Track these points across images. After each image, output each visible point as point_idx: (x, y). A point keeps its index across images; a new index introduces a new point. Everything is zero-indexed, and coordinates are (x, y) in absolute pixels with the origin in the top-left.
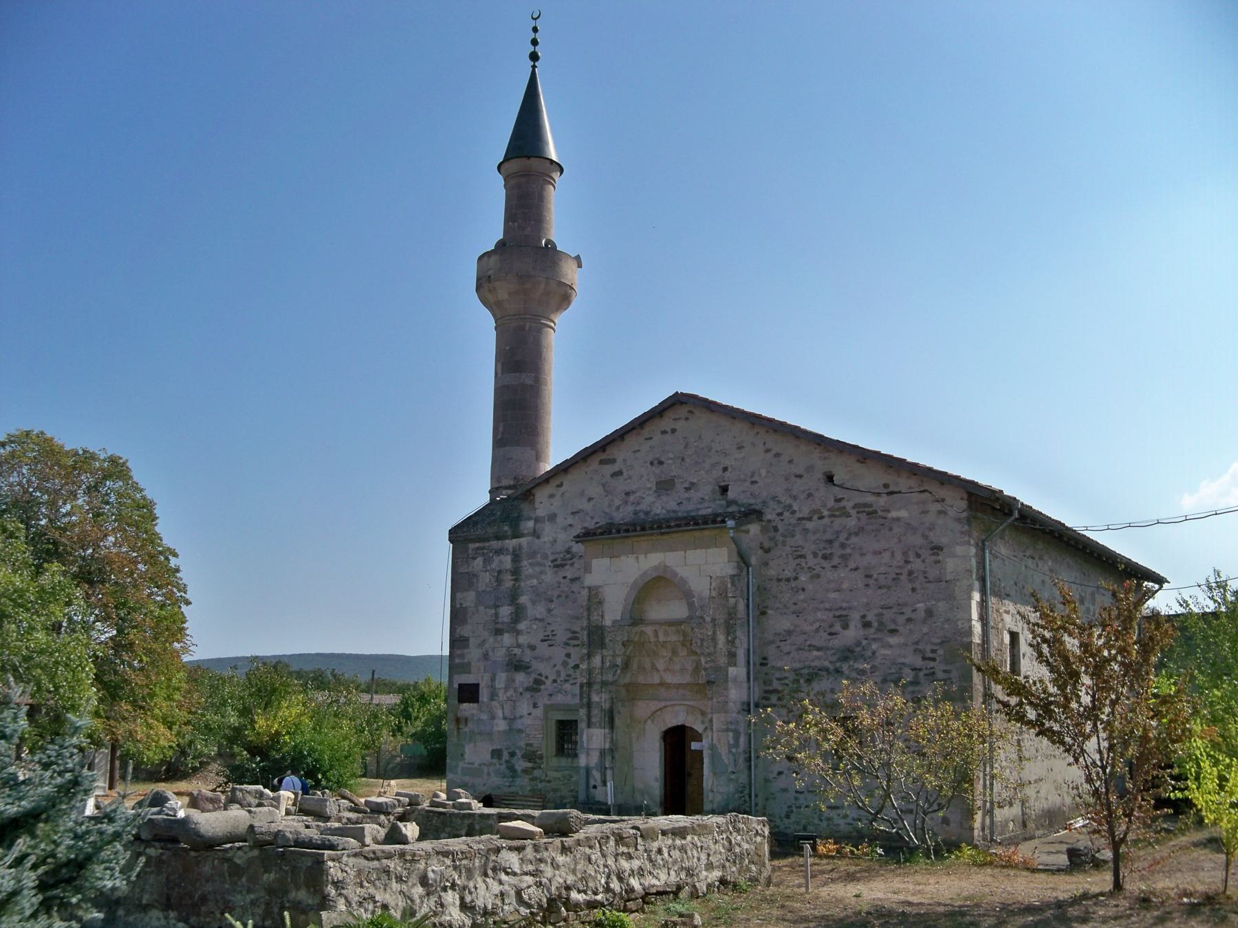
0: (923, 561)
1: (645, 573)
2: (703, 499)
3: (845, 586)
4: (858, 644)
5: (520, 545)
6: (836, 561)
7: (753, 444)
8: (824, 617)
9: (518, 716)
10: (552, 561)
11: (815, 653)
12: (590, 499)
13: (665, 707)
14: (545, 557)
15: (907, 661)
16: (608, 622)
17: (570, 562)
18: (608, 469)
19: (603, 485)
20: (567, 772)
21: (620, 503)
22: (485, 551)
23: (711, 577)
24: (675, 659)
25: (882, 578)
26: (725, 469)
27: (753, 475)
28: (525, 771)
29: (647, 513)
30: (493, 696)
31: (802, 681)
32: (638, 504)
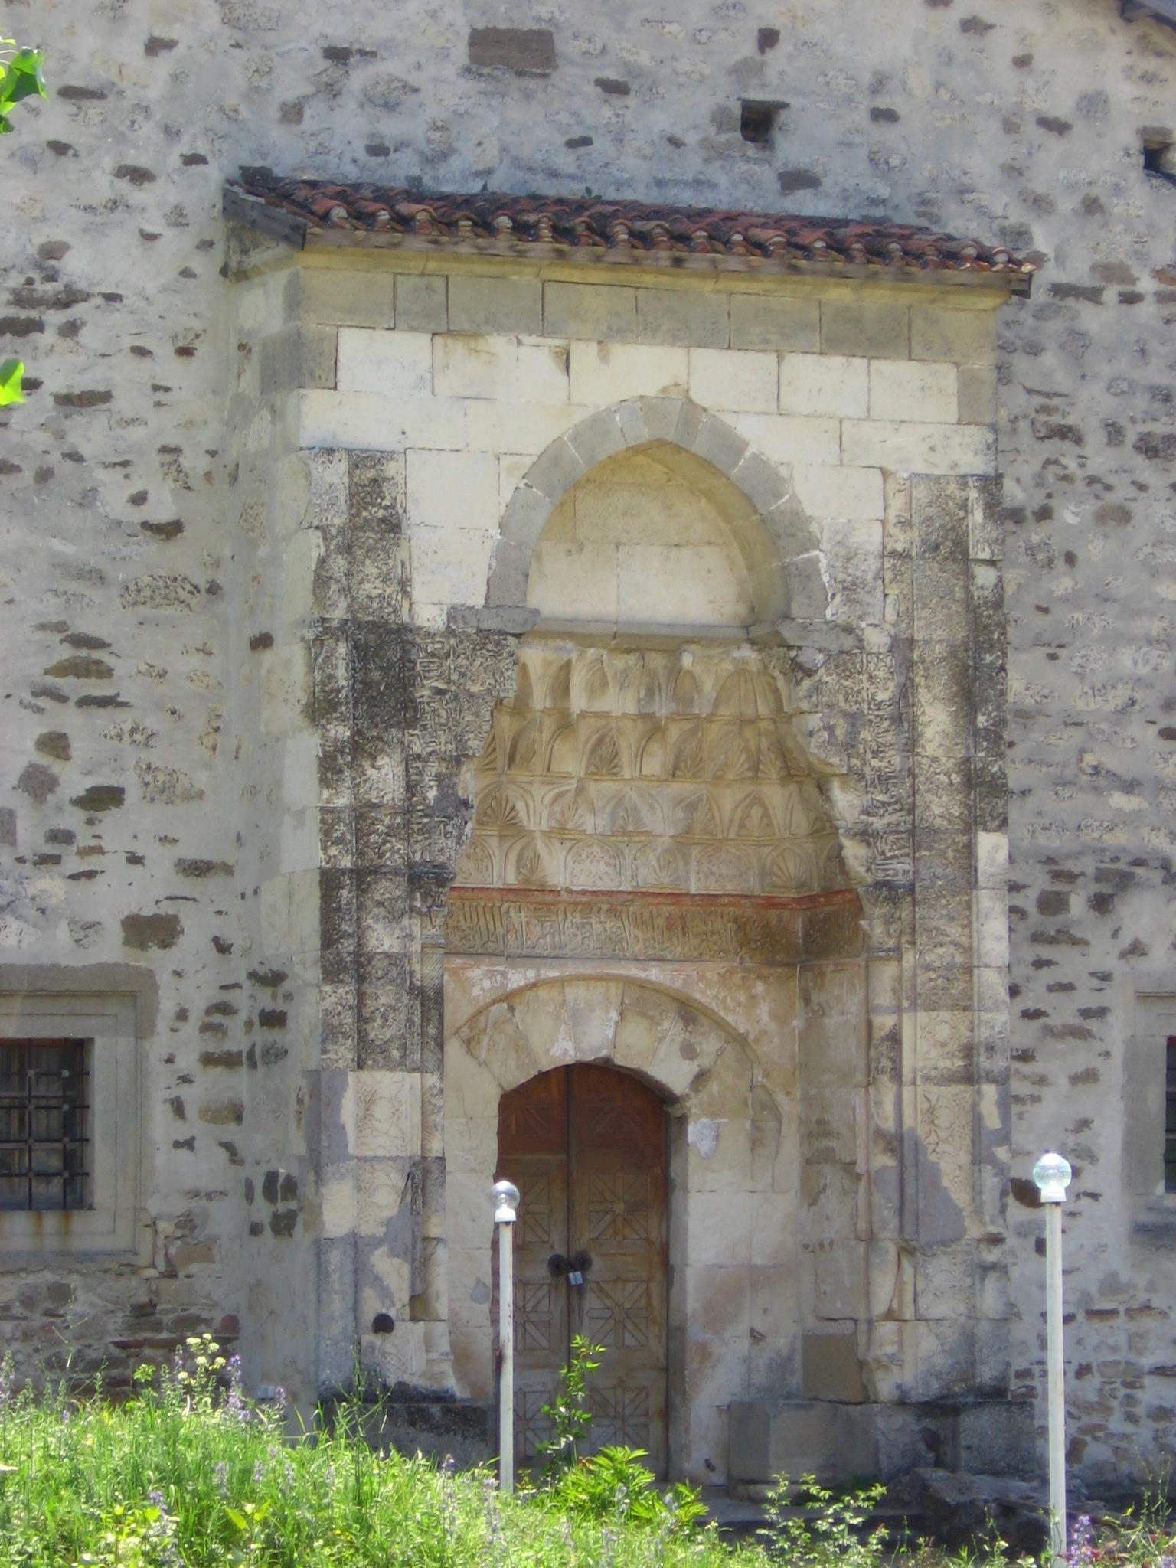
1: (598, 424)
2: (675, 142)
8: (1144, 670)
11: (1119, 800)
12: (155, 46)
13: (533, 986)
17: (55, 318)
20: (49, 1276)
21: (307, 89)
23: (885, 474)
24: (593, 788)
26: (768, 38)
27: (879, 85)
31: (1078, 904)
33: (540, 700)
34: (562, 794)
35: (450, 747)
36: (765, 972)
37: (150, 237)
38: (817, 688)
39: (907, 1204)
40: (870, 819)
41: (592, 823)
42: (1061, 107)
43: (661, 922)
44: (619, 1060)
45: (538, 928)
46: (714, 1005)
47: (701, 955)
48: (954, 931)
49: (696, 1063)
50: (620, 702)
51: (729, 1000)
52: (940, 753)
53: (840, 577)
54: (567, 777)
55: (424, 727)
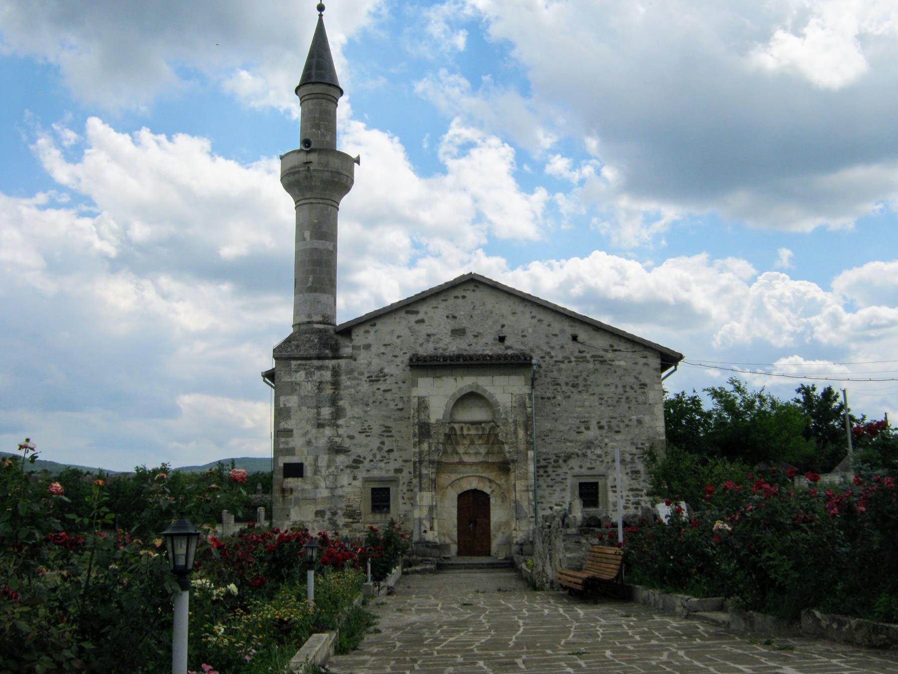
0: (635, 392)
1: (461, 389)
3: (587, 403)
4: (596, 439)
5: (339, 364)
6: (581, 388)
7: (523, 312)
9: (339, 486)
10: (368, 377)
11: (569, 444)
12: (399, 337)
13: (462, 478)
14: (362, 374)
15: (627, 449)
16: (433, 420)
17: (382, 379)
18: (413, 318)
19: (410, 328)
21: (423, 341)
22: (307, 367)
25: (610, 400)
26: (503, 326)
27: (523, 331)
28: (346, 525)
29: (445, 350)
30: (316, 471)
31: (561, 461)
32: (437, 343)
33: (458, 432)
37: (398, 366)
41: (471, 452)
42: (557, 332)
48: (525, 467)
50: (473, 432)
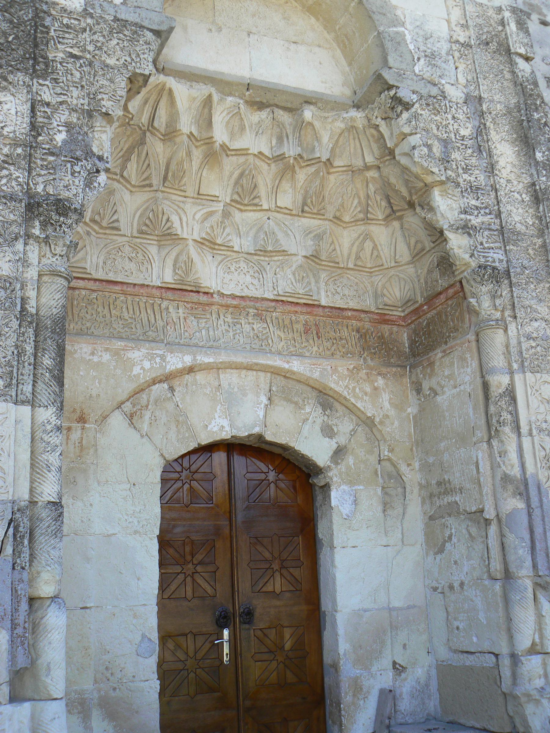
13: (191, 370)
24: (238, 216)
34: (211, 214)
35: (82, 101)
36: (384, 370)
38: (416, 116)
39: (537, 544)
40: (469, 217)
43: (299, 327)
44: (269, 437)
45: (195, 323)
46: (345, 393)
47: (333, 354)
49: (335, 440)
51: (357, 390)
52: (512, 177)
53: (422, 48)
54: (214, 199)
55: (56, 80)
